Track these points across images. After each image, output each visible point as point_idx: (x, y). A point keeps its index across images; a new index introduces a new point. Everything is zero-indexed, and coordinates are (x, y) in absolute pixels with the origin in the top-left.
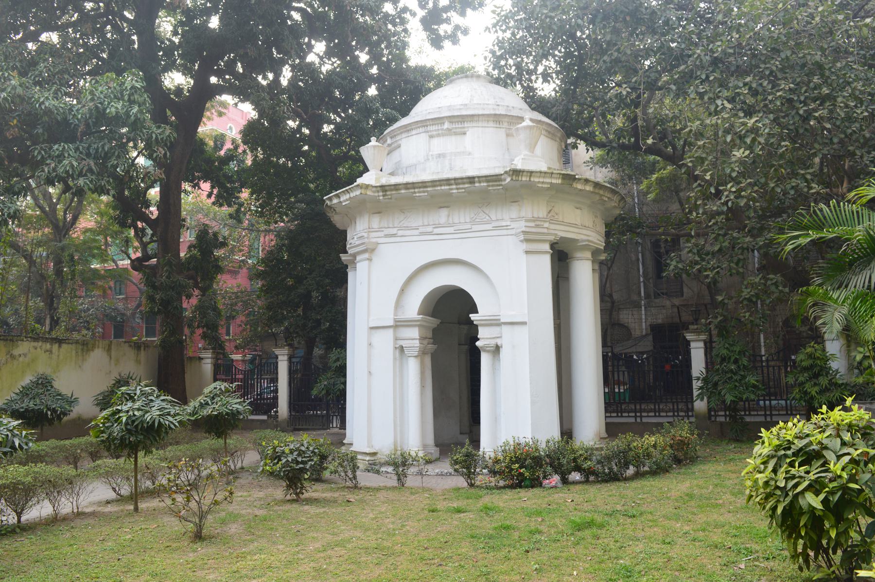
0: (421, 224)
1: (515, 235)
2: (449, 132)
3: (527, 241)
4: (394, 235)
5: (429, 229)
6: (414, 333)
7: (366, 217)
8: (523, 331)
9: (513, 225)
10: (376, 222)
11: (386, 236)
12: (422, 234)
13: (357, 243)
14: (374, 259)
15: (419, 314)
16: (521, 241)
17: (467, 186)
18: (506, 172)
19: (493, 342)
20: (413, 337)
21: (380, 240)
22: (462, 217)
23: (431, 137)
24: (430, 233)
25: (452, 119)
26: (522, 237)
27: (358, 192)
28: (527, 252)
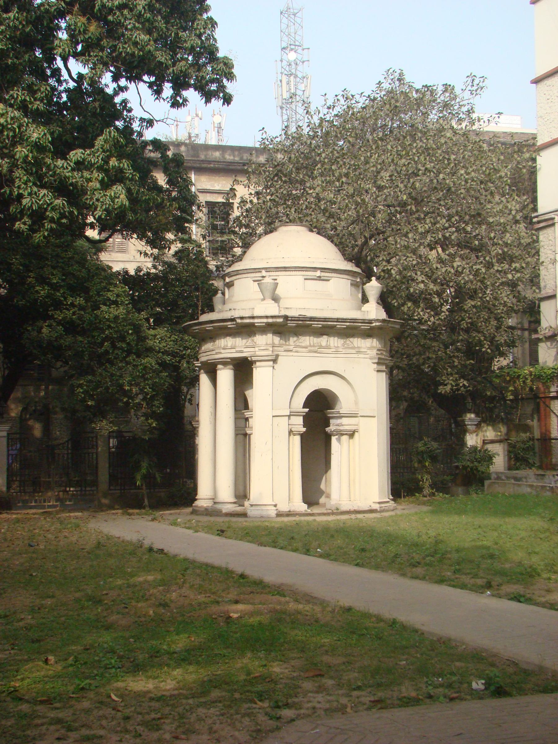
0: (308, 344)
1: (371, 358)
2: (319, 278)
3: (378, 363)
4: (291, 351)
5: (316, 349)
6: (300, 420)
7: (270, 336)
8: (374, 421)
9: (369, 352)
10: (277, 340)
11: (285, 351)
12: (310, 351)
13: (258, 353)
14: (275, 366)
15: (304, 407)
16: (374, 363)
17: (348, 324)
18: (377, 320)
19: (353, 428)
20: (298, 423)
21: (279, 353)
22: (335, 342)
23: (305, 279)
24: (316, 352)
25: (323, 270)
26: (376, 361)
27: (281, 320)
28: (378, 371)
